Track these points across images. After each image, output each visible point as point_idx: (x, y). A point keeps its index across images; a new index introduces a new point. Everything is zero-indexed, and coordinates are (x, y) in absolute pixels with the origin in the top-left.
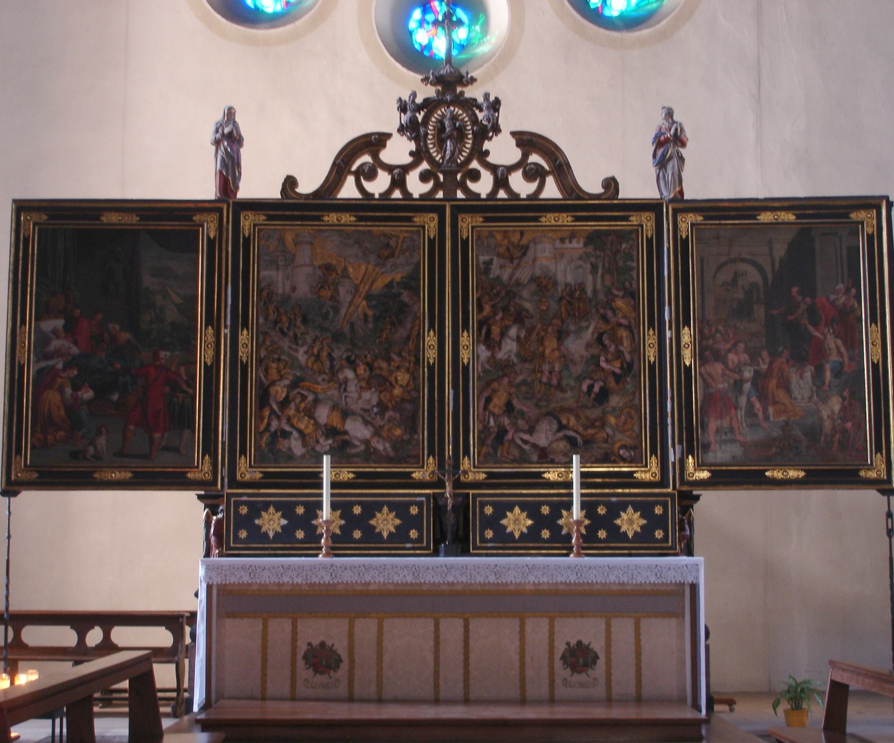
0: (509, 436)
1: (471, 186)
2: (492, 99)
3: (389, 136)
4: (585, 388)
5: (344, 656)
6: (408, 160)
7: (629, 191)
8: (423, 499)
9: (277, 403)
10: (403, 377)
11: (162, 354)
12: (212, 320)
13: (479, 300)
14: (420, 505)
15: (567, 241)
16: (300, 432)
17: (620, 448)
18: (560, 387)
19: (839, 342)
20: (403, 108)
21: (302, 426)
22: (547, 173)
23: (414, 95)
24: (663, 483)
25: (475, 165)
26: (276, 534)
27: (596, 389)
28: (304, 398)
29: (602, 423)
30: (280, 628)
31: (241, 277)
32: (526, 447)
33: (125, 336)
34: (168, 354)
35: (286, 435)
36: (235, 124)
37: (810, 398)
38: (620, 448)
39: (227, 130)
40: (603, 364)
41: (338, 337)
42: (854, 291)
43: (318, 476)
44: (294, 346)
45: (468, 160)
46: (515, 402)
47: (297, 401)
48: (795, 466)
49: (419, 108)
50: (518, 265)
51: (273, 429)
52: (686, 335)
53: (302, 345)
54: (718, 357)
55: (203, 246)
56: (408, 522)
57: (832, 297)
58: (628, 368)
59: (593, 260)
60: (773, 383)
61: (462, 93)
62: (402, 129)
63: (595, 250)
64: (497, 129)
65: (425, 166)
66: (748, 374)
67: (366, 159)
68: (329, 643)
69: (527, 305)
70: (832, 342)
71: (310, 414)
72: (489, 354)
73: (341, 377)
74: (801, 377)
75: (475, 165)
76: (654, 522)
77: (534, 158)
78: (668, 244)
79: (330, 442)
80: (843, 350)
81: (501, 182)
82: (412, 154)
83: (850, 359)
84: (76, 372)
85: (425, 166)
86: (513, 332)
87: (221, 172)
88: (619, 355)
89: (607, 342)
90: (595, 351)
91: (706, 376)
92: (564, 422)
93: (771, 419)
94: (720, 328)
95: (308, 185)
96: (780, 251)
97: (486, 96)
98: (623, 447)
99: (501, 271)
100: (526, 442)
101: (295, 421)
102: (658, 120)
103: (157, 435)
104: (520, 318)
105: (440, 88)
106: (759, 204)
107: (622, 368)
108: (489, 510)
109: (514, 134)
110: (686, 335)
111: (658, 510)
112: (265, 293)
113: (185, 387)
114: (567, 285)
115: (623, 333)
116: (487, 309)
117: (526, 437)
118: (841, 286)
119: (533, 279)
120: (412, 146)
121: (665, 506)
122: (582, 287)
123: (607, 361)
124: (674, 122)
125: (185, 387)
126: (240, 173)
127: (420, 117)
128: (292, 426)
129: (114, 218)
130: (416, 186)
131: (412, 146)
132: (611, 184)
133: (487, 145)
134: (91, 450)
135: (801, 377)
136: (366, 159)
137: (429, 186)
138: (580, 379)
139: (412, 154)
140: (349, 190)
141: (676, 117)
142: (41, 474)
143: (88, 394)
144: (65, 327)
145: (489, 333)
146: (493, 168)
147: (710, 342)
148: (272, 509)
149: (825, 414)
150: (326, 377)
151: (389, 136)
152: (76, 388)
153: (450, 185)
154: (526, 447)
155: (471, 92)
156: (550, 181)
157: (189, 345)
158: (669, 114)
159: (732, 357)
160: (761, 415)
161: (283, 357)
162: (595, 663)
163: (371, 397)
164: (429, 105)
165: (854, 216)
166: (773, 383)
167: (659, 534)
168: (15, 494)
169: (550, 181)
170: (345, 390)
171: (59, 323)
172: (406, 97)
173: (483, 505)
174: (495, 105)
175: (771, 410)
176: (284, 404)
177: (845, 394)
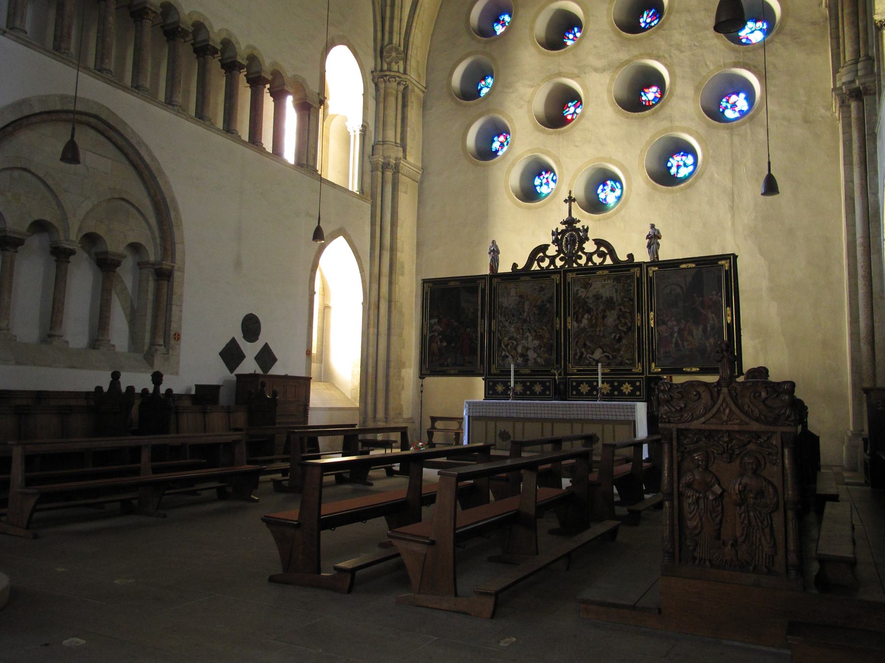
0: (584, 356)
1: (579, 261)
2: (585, 227)
3: (549, 245)
4: (613, 337)
5: (512, 435)
7: (637, 259)
8: (551, 380)
9: (504, 345)
10: (547, 335)
11: (468, 329)
12: (483, 317)
13: (574, 305)
14: (549, 382)
15: (606, 280)
16: (511, 355)
17: (626, 360)
18: (604, 336)
19: (713, 315)
20: (553, 234)
21: (512, 354)
22: (607, 254)
23: (557, 229)
24: (642, 374)
25: (580, 253)
26: (586, 393)
27: (617, 337)
28: (513, 343)
29: (619, 350)
30: (491, 425)
31: (492, 301)
32: (591, 360)
33: (456, 324)
34: (469, 329)
35: (507, 357)
36: (496, 246)
37: (701, 339)
38: (626, 360)
39: (492, 249)
40: (620, 328)
41: (525, 321)
42: (720, 294)
43: (596, 370)
44: (510, 325)
45: (577, 252)
46: (587, 343)
47: (511, 345)
48: (696, 367)
49: (559, 234)
50: (588, 291)
51: (503, 355)
52: (652, 314)
53: (513, 325)
54: (664, 323)
55: (480, 290)
56: (546, 388)
57: (710, 297)
58: (630, 329)
59: (616, 287)
60: (686, 333)
61: (575, 226)
62: (553, 242)
63: (617, 283)
64: (588, 239)
65: (562, 255)
66: (676, 329)
67: (541, 254)
68: (507, 430)
69: (591, 306)
70: (710, 315)
71: (515, 349)
72: (578, 325)
73: (525, 336)
74: (698, 330)
75: (580, 253)
76: (574, 388)
78: (645, 279)
79: (522, 359)
80: (715, 318)
82: (556, 251)
83: (718, 322)
84: (441, 337)
86: (586, 316)
87: (490, 264)
88: (626, 324)
89: (621, 319)
90: (617, 322)
91: (659, 331)
92: (605, 350)
93: (686, 347)
94: (665, 311)
95: (521, 266)
96: (689, 279)
97: (583, 226)
98: (628, 359)
99: (582, 293)
100: (590, 358)
101: (510, 352)
102: (648, 230)
103: (466, 358)
104: (589, 311)
105: (567, 225)
106: (680, 261)
107: (627, 329)
108: (574, 384)
109: (593, 240)
110: (652, 314)
111: (638, 384)
112: (501, 306)
113: (474, 341)
114: (606, 297)
115: (628, 315)
116: (577, 308)
117: (591, 356)
118: (714, 292)
119: (594, 296)
120: (557, 248)
121: (640, 381)
122: (612, 298)
123: (621, 326)
124: (655, 229)
125: (474, 341)
126: (498, 264)
127: (559, 237)
128: (510, 354)
129: (452, 284)
130: (559, 263)
131: (557, 248)
133: (584, 246)
134: (446, 363)
135: (698, 330)
136: (541, 254)
137: (562, 263)
138: (611, 334)
139: (556, 251)
141: (656, 227)
142: (431, 371)
143: (445, 344)
144: (438, 321)
145: (577, 316)
146: (585, 253)
147: (661, 317)
148: (500, 383)
149: (708, 345)
150: (520, 336)
151: (549, 245)
152: (441, 342)
154: (591, 360)
155: (578, 226)
156: (608, 257)
157: (476, 326)
158: (653, 226)
159: (669, 323)
160: (681, 346)
161: (506, 329)
162: (598, 441)
163: (536, 343)
164: (563, 232)
165: (720, 263)
166: (686, 333)
167: (638, 393)
168: (424, 378)
169: (608, 257)
170: (527, 340)
171: (436, 320)
172: (554, 230)
173: (572, 382)
174: (586, 230)
175: (685, 343)
176: (507, 346)
177: (716, 336)
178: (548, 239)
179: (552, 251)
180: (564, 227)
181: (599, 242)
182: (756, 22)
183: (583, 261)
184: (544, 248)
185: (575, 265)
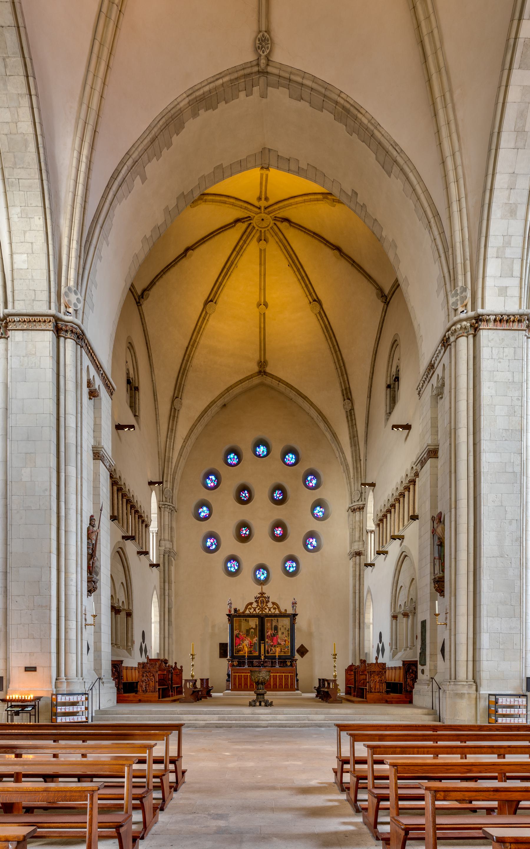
6: (256, 606)
20: (255, 598)
25: (266, 607)
62: (255, 601)
65: (259, 607)
75: (266, 607)
77: (275, 606)
81: (270, 610)
85: (259, 607)
120: (257, 604)
130: (257, 611)
131: (257, 604)
132: (286, 610)
136: (250, 606)
137: (259, 611)
140: (247, 612)
146: (269, 608)
153: (262, 610)
156: (277, 610)
164: (259, 598)
178: (253, 600)
179: (255, 605)
180: (260, 595)
181: (274, 603)
182: (321, 508)
183: (267, 611)
184: (251, 604)
185: (264, 613)
